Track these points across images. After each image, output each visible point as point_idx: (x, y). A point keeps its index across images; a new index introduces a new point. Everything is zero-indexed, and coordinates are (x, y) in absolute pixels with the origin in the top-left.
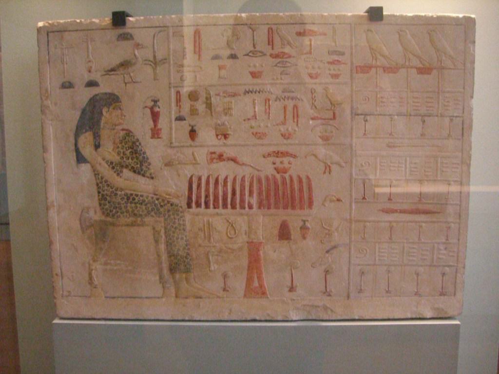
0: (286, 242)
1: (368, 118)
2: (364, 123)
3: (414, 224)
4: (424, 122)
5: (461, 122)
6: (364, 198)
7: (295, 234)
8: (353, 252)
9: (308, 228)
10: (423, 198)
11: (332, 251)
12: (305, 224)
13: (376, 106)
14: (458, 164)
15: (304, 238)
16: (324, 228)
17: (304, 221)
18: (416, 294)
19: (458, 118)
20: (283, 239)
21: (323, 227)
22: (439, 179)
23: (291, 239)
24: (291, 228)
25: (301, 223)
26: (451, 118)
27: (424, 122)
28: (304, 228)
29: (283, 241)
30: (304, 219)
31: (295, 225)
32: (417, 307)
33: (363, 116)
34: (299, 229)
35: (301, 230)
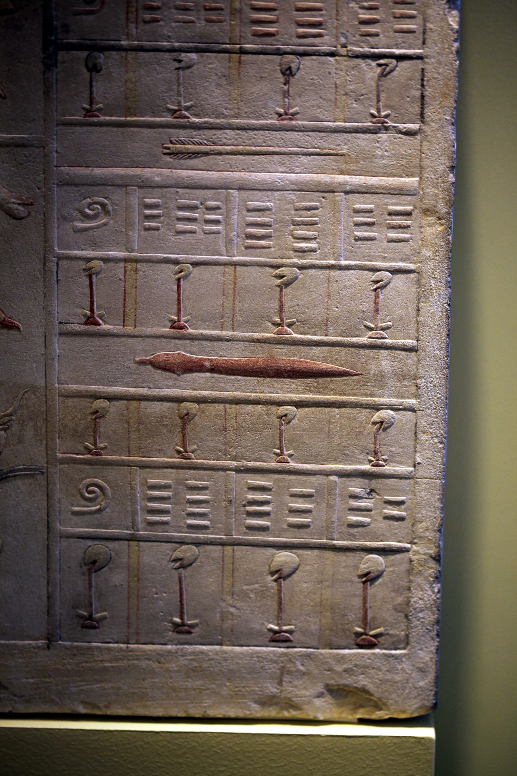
1: (101, 58)
2: (86, 74)
3: (258, 408)
4: (288, 73)
5: (418, 75)
6: (90, 320)
10: (290, 325)
13: (127, 19)
14: (408, 214)
18: (277, 638)
19: (404, 64)
22: (344, 263)
26: (382, 61)
27: (288, 73)
32: (280, 683)
33: (85, 54)
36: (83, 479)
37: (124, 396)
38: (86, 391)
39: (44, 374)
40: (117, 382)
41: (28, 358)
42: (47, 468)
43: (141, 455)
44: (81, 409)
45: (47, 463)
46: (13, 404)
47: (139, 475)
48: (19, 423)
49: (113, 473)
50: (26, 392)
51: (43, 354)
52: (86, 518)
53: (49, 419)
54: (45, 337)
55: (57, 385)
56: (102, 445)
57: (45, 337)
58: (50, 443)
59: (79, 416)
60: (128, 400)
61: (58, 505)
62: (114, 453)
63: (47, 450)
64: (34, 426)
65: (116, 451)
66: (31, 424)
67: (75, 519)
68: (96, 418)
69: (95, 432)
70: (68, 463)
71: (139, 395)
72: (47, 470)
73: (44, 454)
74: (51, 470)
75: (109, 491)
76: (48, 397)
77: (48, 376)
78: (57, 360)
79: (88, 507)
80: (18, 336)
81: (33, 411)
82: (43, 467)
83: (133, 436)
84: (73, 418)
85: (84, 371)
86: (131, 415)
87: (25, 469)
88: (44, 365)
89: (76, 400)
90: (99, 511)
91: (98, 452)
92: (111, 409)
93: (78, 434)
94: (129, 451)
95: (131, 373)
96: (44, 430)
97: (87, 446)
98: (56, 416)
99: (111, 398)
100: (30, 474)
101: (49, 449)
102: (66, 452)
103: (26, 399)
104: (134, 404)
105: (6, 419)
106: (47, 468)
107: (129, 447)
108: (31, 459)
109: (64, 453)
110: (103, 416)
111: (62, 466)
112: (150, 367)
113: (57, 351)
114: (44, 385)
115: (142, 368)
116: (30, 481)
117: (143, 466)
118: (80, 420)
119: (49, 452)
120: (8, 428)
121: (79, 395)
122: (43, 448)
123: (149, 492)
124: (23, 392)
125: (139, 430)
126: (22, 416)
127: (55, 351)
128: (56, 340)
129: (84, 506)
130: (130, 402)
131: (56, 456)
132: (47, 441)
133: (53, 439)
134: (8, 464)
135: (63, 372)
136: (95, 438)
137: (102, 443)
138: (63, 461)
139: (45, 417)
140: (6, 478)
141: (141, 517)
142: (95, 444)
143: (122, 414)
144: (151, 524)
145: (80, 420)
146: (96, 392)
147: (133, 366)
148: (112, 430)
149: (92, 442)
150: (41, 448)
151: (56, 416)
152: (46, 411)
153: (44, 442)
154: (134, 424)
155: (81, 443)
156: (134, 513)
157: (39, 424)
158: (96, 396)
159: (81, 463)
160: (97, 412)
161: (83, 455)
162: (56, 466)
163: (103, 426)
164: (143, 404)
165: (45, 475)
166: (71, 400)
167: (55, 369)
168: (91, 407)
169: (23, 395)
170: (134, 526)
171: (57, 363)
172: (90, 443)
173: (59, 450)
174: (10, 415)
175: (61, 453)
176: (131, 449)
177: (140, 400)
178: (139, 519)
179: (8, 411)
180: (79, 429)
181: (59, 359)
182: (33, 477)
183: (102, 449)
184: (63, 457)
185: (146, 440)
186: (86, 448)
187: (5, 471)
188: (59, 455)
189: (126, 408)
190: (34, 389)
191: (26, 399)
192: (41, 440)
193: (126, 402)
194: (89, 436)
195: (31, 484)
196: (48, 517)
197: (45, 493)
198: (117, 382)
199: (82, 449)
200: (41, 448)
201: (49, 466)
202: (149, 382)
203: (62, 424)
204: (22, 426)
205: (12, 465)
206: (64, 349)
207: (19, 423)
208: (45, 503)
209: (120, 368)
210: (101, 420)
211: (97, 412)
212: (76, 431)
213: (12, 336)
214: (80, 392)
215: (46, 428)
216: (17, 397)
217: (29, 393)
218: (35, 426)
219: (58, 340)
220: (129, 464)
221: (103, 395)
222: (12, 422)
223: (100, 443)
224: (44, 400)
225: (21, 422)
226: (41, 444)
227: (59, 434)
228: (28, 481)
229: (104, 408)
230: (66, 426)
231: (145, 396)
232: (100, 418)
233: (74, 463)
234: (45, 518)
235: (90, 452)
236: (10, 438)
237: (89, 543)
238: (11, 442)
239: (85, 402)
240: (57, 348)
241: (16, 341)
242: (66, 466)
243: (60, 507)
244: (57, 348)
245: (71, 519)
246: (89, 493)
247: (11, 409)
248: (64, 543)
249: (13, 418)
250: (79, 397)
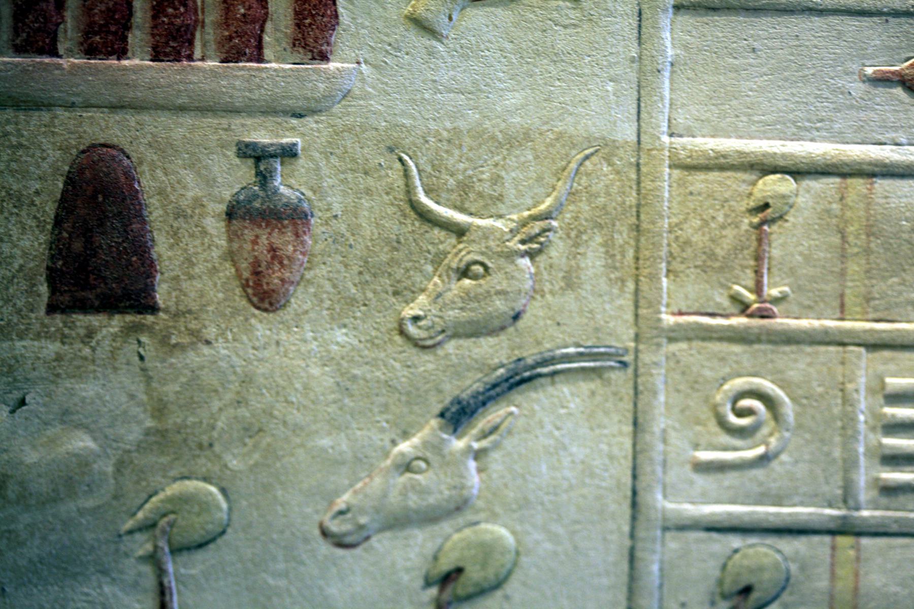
0: (110, 326)
7: (190, 258)
8: (661, 418)
9: (295, 217)
11: (494, 414)
12: (264, 178)
15: (264, 295)
16: (425, 216)
17: (257, 155)
20: (84, 307)
21: (415, 206)
23: (153, 309)
24: (155, 212)
25: (233, 178)
28: (264, 216)
29: (82, 320)
30: (263, 138)
31: (187, 185)
34: (215, 226)
35: (232, 236)
36: (725, 380)
37: (834, 165)
38: (740, 153)
39: (634, 111)
40: (818, 129)
41: (597, 70)
42: (637, 351)
43: (871, 316)
44: (726, 201)
45: (637, 338)
46: (554, 188)
47: (864, 367)
48: (569, 236)
49: (800, 364)
50: (587, 157)
51: (633, 60)
52: (731, 479)
53: (644, 226)
54: (640, 14)
55: (666, 139)
56: (775, 292)
57: (640, 14)
58: (644, 287)
59: (721, 219)
60: (844, 175)
61: (660, 447)
62: (807, 310)
63: (637, 307)
64: (605, 244)
65: (810, 307)
66: (599, 239)
67: (702, 481)
68: (763, 222)
69: (758, 258)
70: (689, 339)
71: (870, 164)
72: (636, 358)
73: (629, 317)
74: (646, 357)
75: (789, 408)
76: (644, 169)
77: (643, 115)
78: (667, 74)
79: (735, 449)
80: (572, 14)
81: (604, 207)
82: (626, 350)
83: (853, 267)
84: (706, 223)
85: (734, 102)
86: (849, 214)
87: (581, 354)
88: (635, 86)
89: (714, 176)
90: (764, 460)
91: (767, 309)
92: (800, 200)
93: (717, 265)
94: (842, 306)
95: (852, 107)
96: (631, 253)
97: (739, 294)
98: (662, 217)
99: (798, 171)
100: (593, 370)
101: (642, 302)
102: (684, 310)
103: (588, 175)
104: (858, 185)
105: (537, 227)
106: (637, 351)
107: (842, 296)
108: (597, 330)
109: (681, 314)
110: (781, 217)
111: (674, 347)
112: (899, 91)
113: (670, 52)
114: (634, 138)
115: (881, 92)
116: (592, 386)
117: (875, 345)
118: (723, 227)
119: (642, 312)
120: (540, 251)
121: (720, 164)
122: (627, 302)
123: (889, 411)
124: (580, 156)
125: (868, 251)
126: (576, 218)
127: (663, 53)
128: (668, 22)
129: (725, 449)
130: (849, 181)
131: (659, 320)
132: (637, 282)
133: (654, 278)
134: (539, 343)
135: (683, 105)
136: (758, 273)
137: (775, 285)
138: (674, 335)
139: (634, 220)
140: (530, 379)
141: (868, 473)
142: (758, 289)
143: (828, 211)
144: (890, 490)
145: (723, 227)
146: (765, 155)
147: (858, 88)
148: (801, 254)
149: (751, 283)
150: (621, 302)
151: (662, 217)
152: (639, 206)
153: (631, 286)
154: (857, 237)
155: (722, 286)
156: (850, 464)
157: (619, 240)
158: (764, 167)
159: (720, 339)
160: (767, 206)
161: (726, 316)
162: (659, 345)
163: (782, 242)
164: (882, 185)
165: (630, 371)
166: (701, 176)
167: (662, 99)
168: (751, 194)
169: (581, 164)
170: (847, 497)
171: (667, 84)
172: (745, 287)
173: (668, 306)
174: (546, 216)
175: (673, 314)
176: (847, 300)
177: (873, 175)
178: (862, 479)
179: (543, 207)
180: (718, 251)
181: (672, 72)
182: (600, 377)
183: (776, 301)
184: (678, 325)
185: (884, 279)
186: (735, 299)
187: (530, 361)
188: (669, 319)
189: (837, 197)
190: (605, 148)
191: (588, 175)
192: (623, 281)
193: (838, 180)
194: (743, 267)
195: (593, 393)
196: (635, 477)
197: (630, 416)
198: (818, 129)
199: (726, 303)
200: (621, 302)
201: (641, 347)
202: (896, 129)
203: (677, 238)
204: (576, 245)
205: (548, 346)
206: (686, 47)
207: (569, 236)
208: (628, 443)
209: (826, 94)
210: (775, 228)
211: (767, 206)
212: (712, 256)
213: (555, 15)
214: (724, 157)
215: (637, 250)
216: (564, 169)
217: (594, 159)
218: (608, 244)
219: (672, 22)
220: (840, 341)
221: (782, 163)
222: (550, 234)
223: (769, 288)
224: (634, 176)
225: (573, 234)
226: (622, 290)
227: (669, 263)
228: (585, 386)
229: (784, 197)
230: (688, 243)
231: (885, 165)
232: (773, 221)
233: (704, 339)
234: (627, 480)
235: (744, 308)
236: (546, 276)
237: (735, 541)
238: (547, 287)
239: (736, 182)
240: (668, 43)
241: (565, 27)
242: (683, 345)
243: (665, 453)
244: (668, 43)
245: (692, 483)
246: (740, 413)
247: (549, 201)
248: (674, 543)
249: (555, 223)
250: (722, 168)
